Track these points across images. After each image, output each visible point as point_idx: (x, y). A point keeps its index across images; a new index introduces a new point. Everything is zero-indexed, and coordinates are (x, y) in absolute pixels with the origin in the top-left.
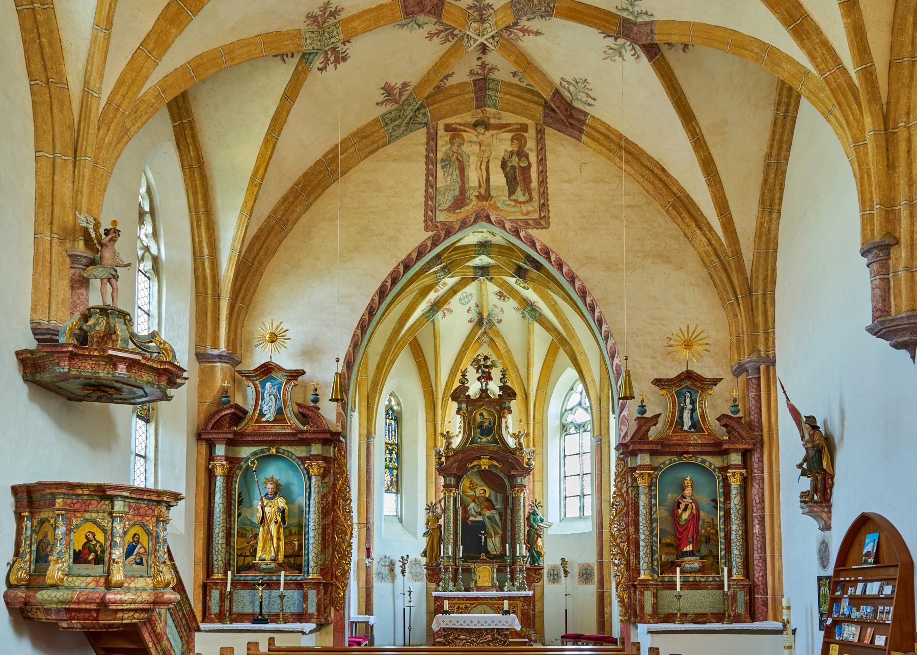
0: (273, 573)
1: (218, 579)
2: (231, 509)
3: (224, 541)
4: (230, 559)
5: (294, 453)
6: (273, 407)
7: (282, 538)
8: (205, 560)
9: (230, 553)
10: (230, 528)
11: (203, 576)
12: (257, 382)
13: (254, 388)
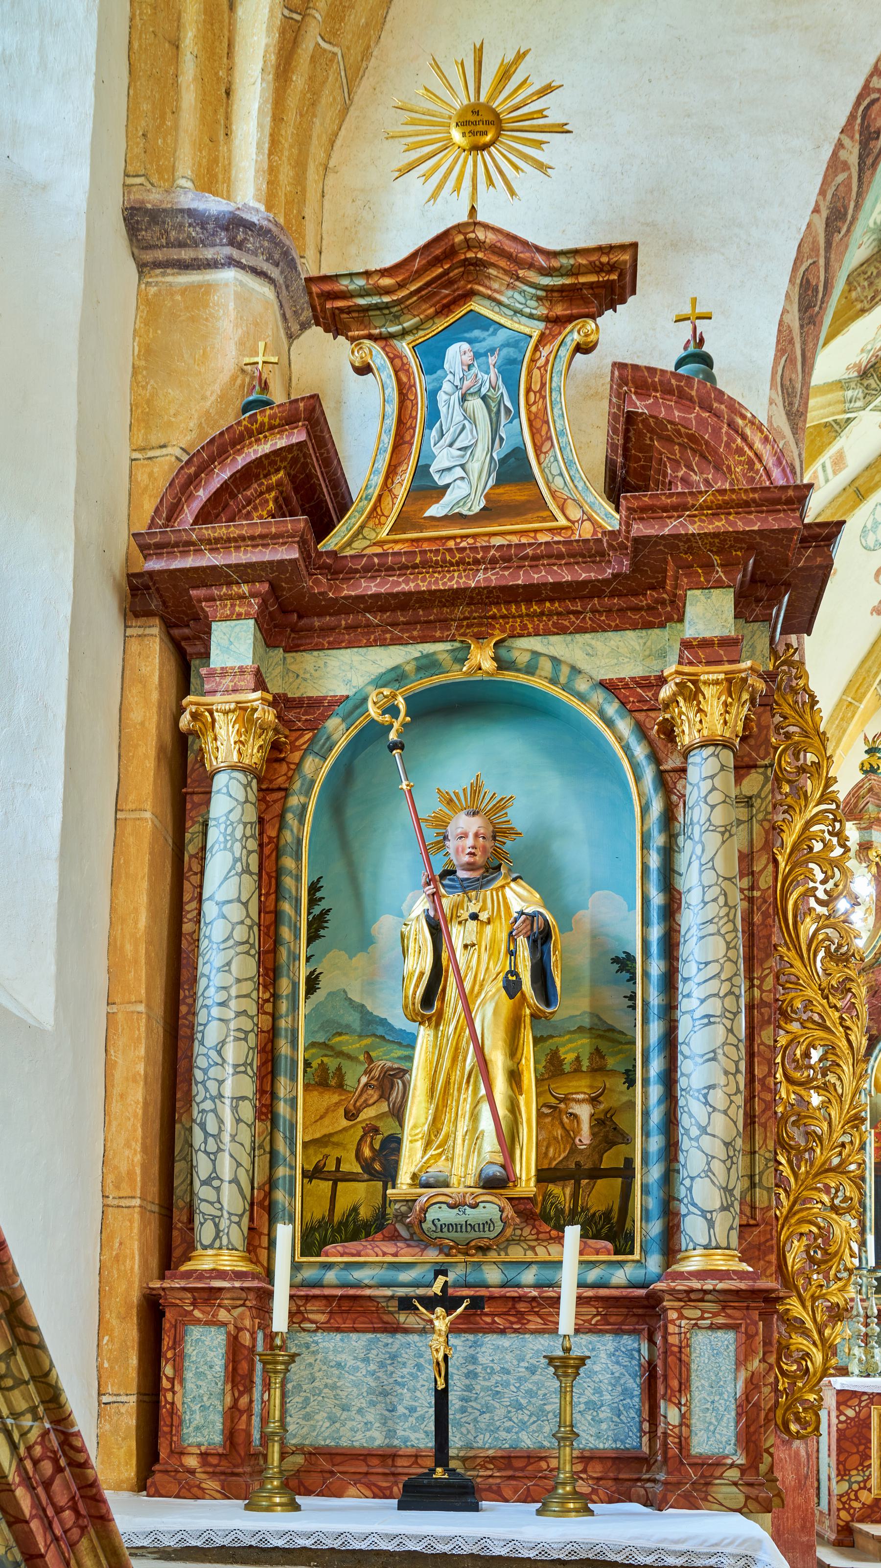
0: (484, 1250)
1: (221, 1274)
2: (277, 941)
3: (248, 1087)
4: (271, 1183)
5: (582, 665)
6: (481, 452)
7: (529, 1079)
8: (154, 1190)
9: (273, 1154)
10: (273, 1033)
11: (144, 1264)
12: (404, 347)
13: (393, 392)
